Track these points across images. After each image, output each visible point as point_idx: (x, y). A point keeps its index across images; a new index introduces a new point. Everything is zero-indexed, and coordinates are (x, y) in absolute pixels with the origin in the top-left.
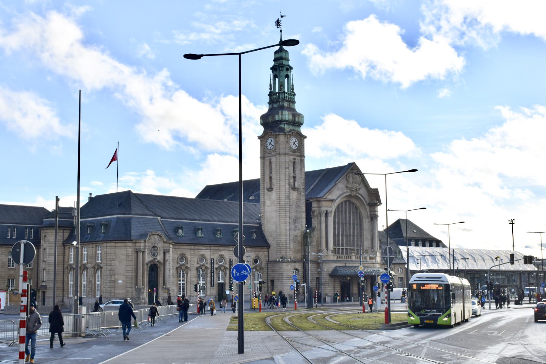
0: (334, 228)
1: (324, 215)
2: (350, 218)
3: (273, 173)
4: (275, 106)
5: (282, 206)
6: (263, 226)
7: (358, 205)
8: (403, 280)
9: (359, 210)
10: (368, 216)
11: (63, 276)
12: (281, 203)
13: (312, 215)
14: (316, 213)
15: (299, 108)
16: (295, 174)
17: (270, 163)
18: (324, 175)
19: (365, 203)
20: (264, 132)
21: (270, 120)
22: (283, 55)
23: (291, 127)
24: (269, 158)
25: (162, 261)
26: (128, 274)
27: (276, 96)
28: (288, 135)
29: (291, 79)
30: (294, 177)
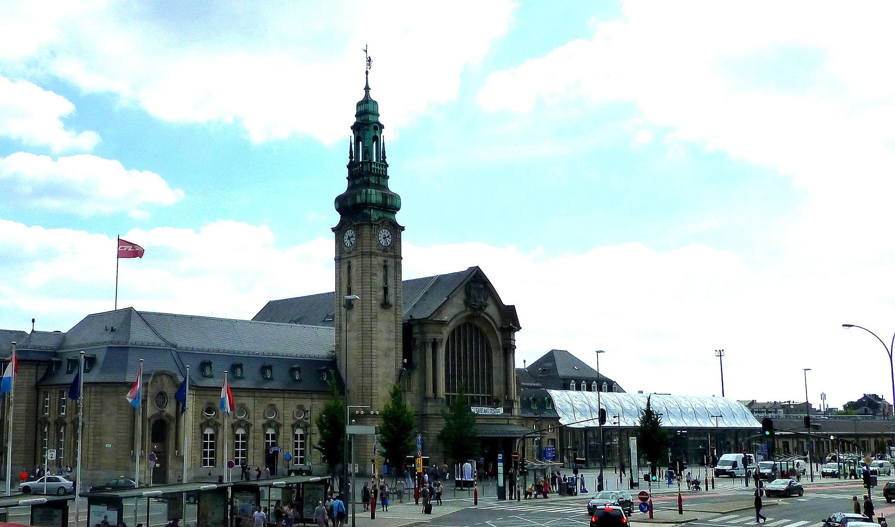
1: (430, 345)
3: (353, 281)
4: (357, 182)
7: (485, 329)
8: (555, 444)
9: (485, 338)
11: (36, 434)
12: (364, 326)
14: (418, 342)
15: (394, 185)
16: (386, 284)
17: (349, 267)
18: (434, 285)
21: (349, 202)
22: (370, 107)
23: (381, 214)
24: (348, 260)
25: (173, 415)
26: (120, 434)
27: (358, 168)
28: (375, 225)
29: (382, 143)
30: (386, 290)
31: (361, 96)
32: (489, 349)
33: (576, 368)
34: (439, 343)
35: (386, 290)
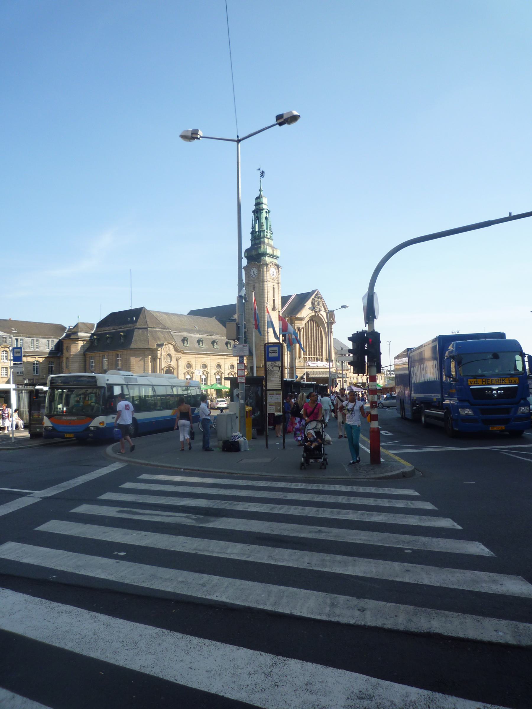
4: (257, 242)
6: (248, 339)
20: (248, 263)
21: (254, 253)
25: (175, 367)
30: (274, 300)
31: (258, 195)
35: (274, 300)
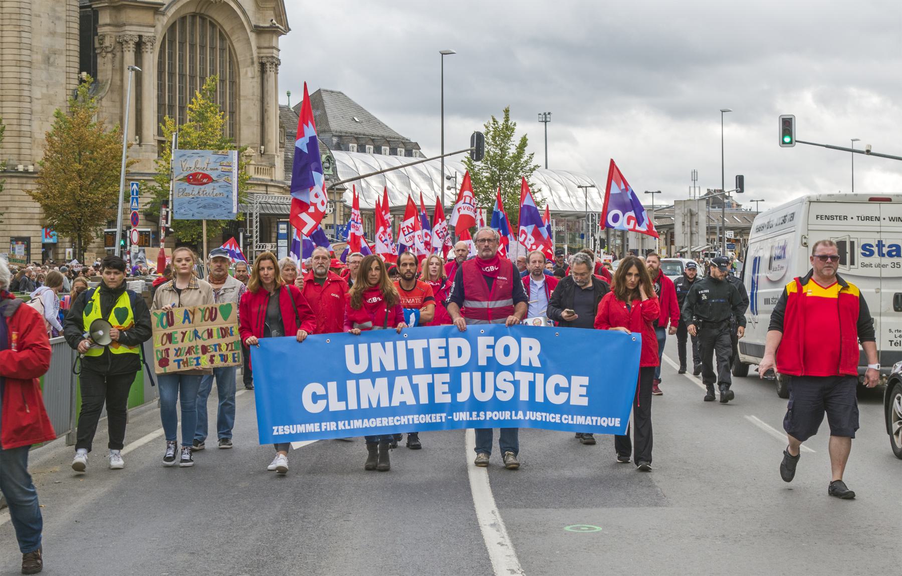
0: (161, 87)
1: (132, 45)
2: (203, 61)
5: (7, 16)
9: (228, 42)
10: (252, 59)
13: (97, 45)
14: (107, 42)
19: (245, 23)
32: (233, 63)
33: (356, 119)
34: (149, 44)
